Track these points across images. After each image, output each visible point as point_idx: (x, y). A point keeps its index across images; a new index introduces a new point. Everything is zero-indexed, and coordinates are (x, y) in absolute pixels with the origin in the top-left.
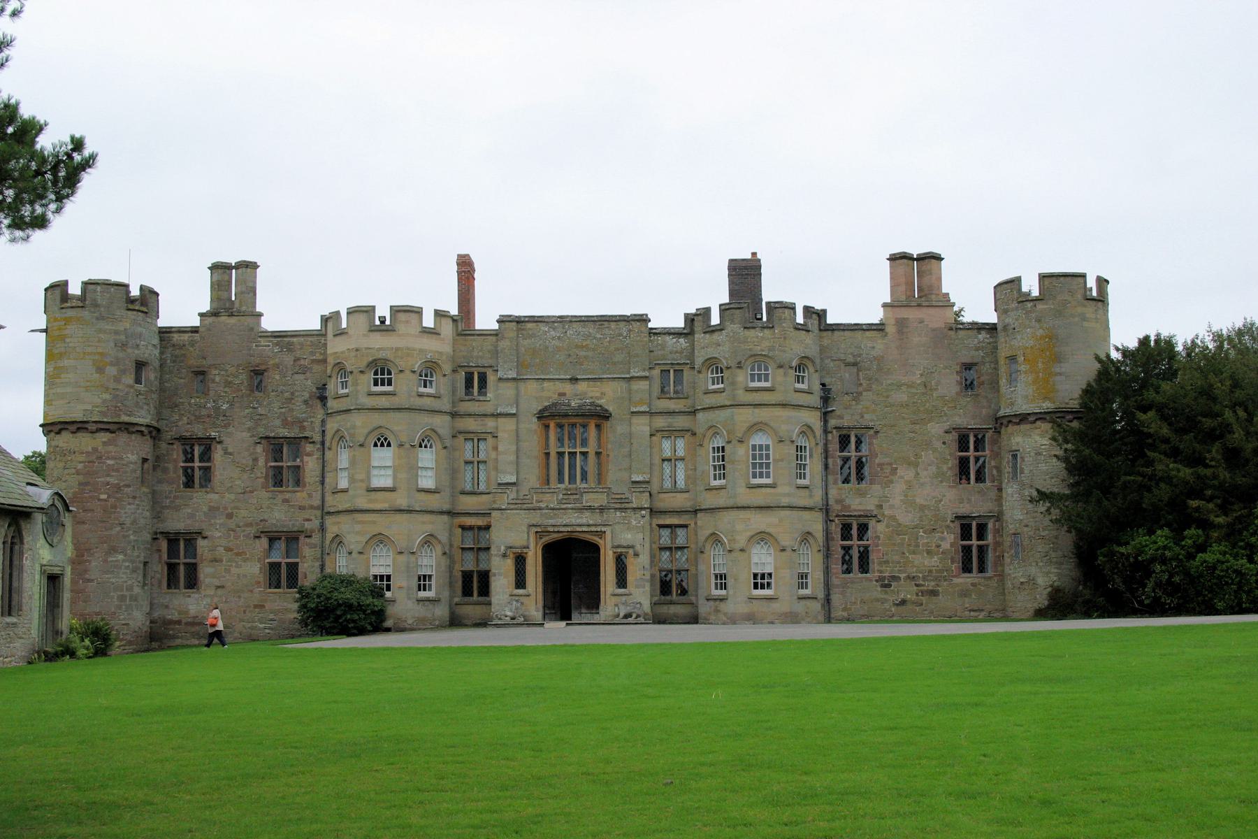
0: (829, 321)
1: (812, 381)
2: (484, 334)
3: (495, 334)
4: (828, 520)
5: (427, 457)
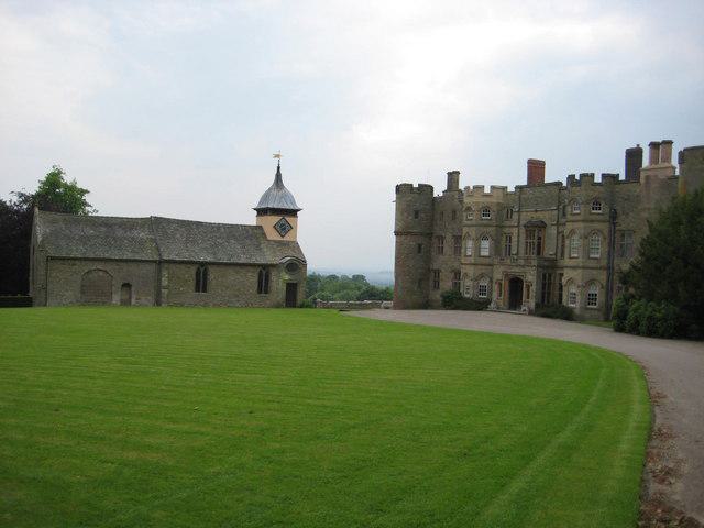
0: (621, 179)
1: (605, 209)
2: (511, 193)
3: (515, 193)
4: (610, 276)
5: (486, 244)
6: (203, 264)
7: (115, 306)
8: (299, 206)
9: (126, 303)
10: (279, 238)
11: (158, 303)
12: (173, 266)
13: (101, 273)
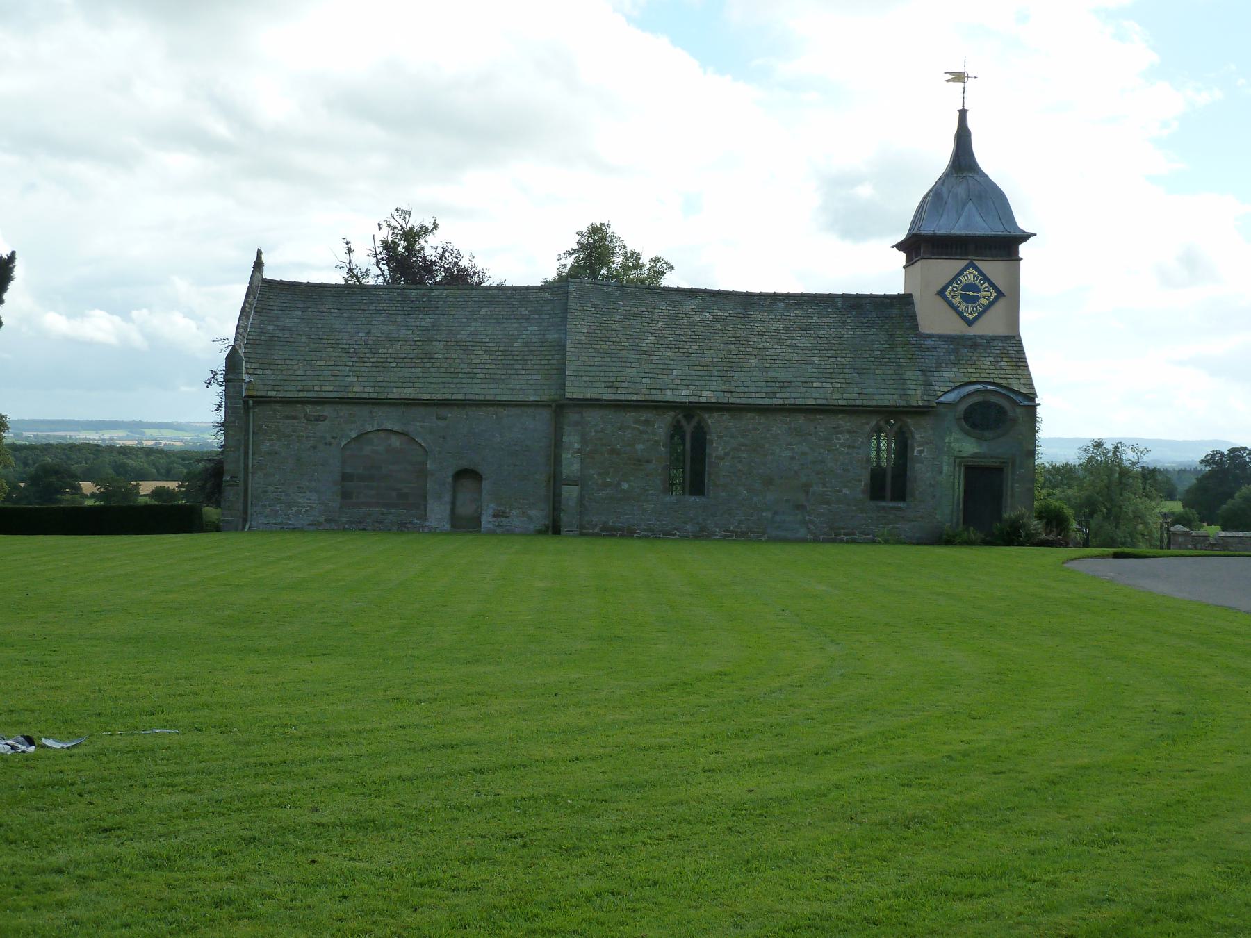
6: (689, 410)
7: (433, 531)
8: (1023, 222)
9: (464, 524)
10: (949, 325)
11: (554, 528)
12: (594, 417)
13: (395, 442)
